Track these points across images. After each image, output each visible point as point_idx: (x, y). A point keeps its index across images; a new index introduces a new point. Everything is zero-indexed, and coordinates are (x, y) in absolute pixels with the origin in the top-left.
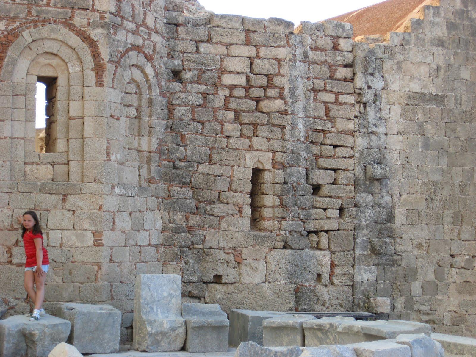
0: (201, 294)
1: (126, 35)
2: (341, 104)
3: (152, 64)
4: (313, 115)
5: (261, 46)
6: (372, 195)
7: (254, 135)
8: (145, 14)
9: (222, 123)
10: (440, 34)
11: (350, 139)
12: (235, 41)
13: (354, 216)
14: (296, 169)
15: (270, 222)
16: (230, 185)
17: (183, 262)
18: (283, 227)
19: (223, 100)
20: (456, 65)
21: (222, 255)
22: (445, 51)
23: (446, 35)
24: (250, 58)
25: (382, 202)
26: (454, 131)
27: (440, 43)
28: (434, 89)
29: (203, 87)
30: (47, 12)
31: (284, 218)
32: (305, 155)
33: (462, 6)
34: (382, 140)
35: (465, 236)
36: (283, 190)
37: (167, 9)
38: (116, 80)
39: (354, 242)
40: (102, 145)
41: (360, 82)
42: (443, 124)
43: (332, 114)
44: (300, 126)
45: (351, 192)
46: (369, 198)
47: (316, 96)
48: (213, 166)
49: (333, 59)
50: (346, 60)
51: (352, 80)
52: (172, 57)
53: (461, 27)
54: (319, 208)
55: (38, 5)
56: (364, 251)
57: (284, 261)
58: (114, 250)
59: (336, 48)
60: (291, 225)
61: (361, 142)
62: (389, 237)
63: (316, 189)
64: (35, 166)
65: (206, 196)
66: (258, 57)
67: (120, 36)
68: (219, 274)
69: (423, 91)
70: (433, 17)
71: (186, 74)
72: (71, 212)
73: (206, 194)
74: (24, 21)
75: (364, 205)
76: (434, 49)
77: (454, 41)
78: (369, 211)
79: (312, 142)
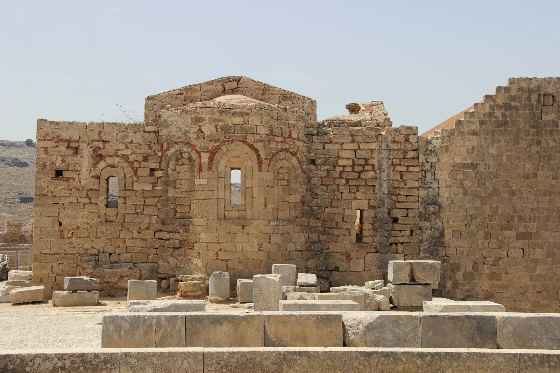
0: (328, 277)
1: (277, 144)
2: (410, 172)
3: (296, 157)
4: (392, 179)
5: (361, 143)
6: (430, 222)
7: (357, 192)
8: (290, 131)
9: (338, 186)
10: (475, 128)
11: (416, 191)
12: (345, 141)
13: (418, 235)
14: (381, 209)
15: (367, 238)
16: (343, 219)
17: (317, 259)
18: (375, 241)
19: (339, 174)
20: (486, 145)
21: (339, 256)
22: (478, 138)
23: (479, 128)
24: (354, 150)
25: (436, 226)
26: (485, 184)
27: (474, 133)
28: (470, 160)
29: (328, 167)
30: (233, 136)
31: (375, 236)
32: (387, 201)
33: (490, 110)
34: (436, 191)
35: (493, 246)
36: (374, 221)
37: (306, 127)
38: (270, 168)
39: (419, 249)
40: (262, 201)
41: (422, 158)
42: (476, 181)
43: (404, 178)
44: (385, 185)
45: (416, 221)
46: (428, 224)
47: (395, 168)
48: (333, 209)
49: (405, 147)
50: (414, 147)
51: (418, 158)
52: (310, 152)
53: (489, 123)
54: (397, 230)
55: (229, 133)
56: (425, 254)
57: (375, 259)
58: (270, 253)
59: (407, 140)
60: (379, 240)
61: (422, 192)
62: (441, 246)
63: (395, 220)
64: (230, 212)
65: (329, 224)
66: (359, 149)
67: (273, 145)
68: (337, 266)
69: (463, 162)
70: (470, 119)
71: (317, 161)
72: (247, 234)
73: (329, 224)
74: (222, 141)
75: (425, 228)
76: (471, 137)
77: (484, 131)
78: (428, 232)
79: (392, 194)
